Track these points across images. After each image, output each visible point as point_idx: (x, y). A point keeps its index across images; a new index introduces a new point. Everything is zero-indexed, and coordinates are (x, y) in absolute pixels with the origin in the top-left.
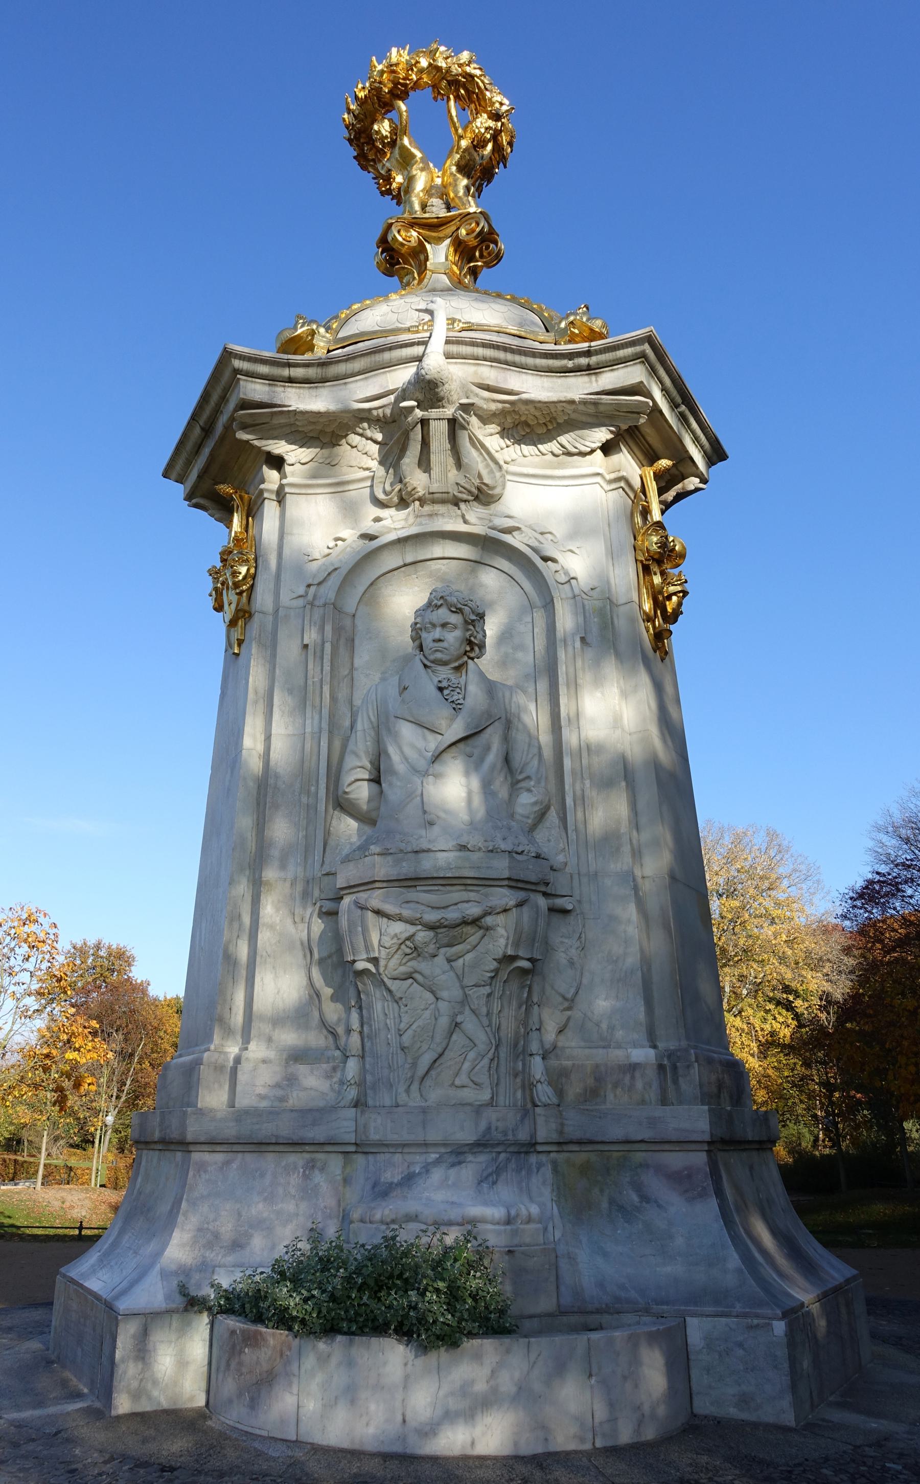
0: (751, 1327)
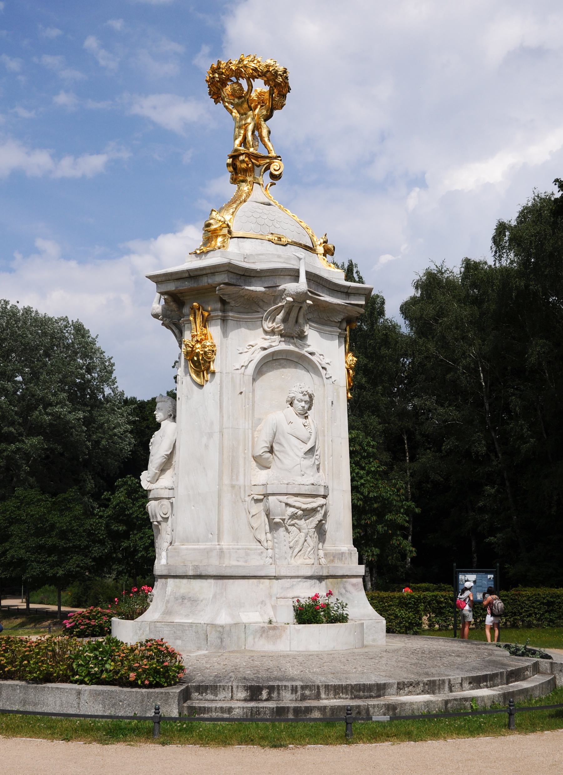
0: (377, 622)
